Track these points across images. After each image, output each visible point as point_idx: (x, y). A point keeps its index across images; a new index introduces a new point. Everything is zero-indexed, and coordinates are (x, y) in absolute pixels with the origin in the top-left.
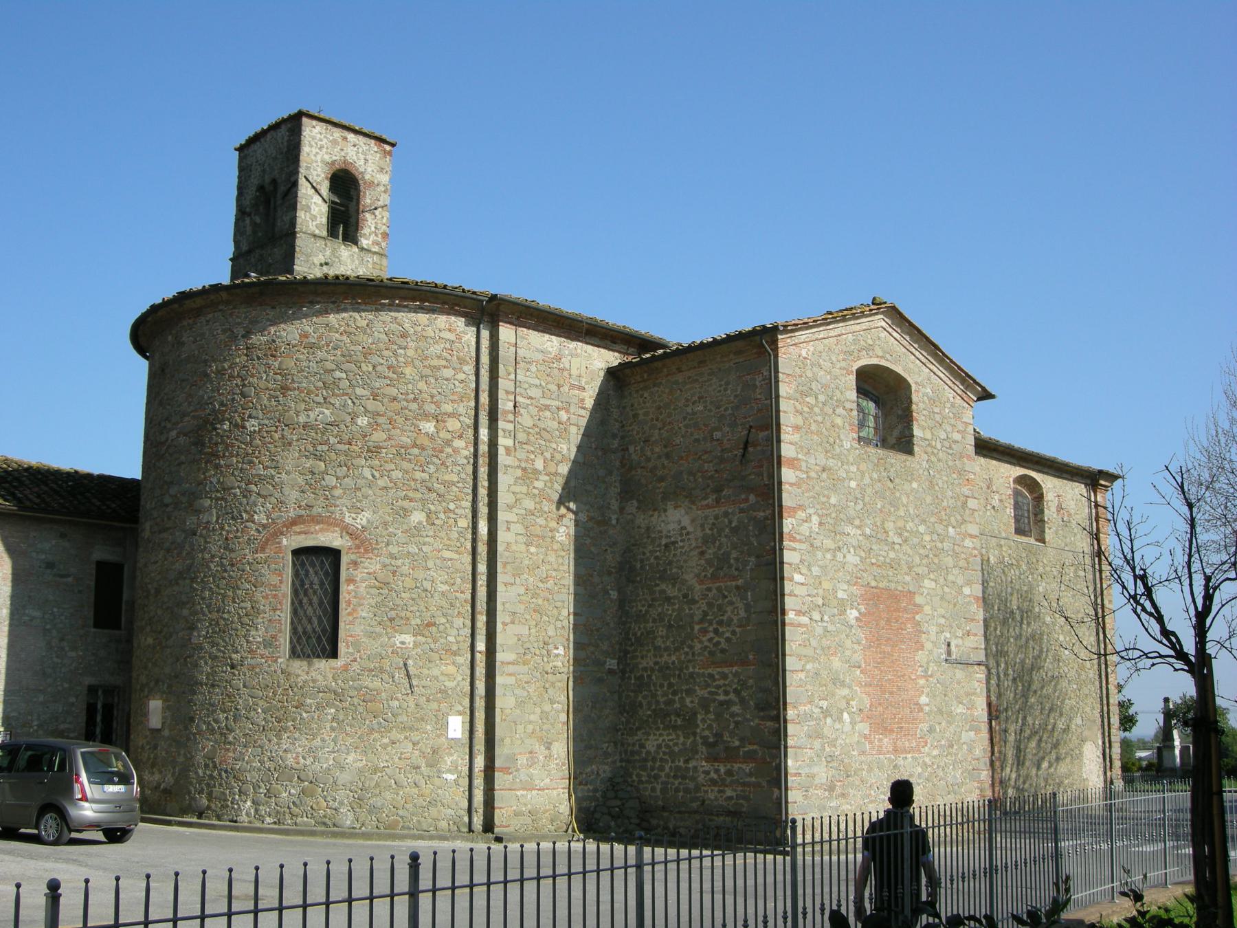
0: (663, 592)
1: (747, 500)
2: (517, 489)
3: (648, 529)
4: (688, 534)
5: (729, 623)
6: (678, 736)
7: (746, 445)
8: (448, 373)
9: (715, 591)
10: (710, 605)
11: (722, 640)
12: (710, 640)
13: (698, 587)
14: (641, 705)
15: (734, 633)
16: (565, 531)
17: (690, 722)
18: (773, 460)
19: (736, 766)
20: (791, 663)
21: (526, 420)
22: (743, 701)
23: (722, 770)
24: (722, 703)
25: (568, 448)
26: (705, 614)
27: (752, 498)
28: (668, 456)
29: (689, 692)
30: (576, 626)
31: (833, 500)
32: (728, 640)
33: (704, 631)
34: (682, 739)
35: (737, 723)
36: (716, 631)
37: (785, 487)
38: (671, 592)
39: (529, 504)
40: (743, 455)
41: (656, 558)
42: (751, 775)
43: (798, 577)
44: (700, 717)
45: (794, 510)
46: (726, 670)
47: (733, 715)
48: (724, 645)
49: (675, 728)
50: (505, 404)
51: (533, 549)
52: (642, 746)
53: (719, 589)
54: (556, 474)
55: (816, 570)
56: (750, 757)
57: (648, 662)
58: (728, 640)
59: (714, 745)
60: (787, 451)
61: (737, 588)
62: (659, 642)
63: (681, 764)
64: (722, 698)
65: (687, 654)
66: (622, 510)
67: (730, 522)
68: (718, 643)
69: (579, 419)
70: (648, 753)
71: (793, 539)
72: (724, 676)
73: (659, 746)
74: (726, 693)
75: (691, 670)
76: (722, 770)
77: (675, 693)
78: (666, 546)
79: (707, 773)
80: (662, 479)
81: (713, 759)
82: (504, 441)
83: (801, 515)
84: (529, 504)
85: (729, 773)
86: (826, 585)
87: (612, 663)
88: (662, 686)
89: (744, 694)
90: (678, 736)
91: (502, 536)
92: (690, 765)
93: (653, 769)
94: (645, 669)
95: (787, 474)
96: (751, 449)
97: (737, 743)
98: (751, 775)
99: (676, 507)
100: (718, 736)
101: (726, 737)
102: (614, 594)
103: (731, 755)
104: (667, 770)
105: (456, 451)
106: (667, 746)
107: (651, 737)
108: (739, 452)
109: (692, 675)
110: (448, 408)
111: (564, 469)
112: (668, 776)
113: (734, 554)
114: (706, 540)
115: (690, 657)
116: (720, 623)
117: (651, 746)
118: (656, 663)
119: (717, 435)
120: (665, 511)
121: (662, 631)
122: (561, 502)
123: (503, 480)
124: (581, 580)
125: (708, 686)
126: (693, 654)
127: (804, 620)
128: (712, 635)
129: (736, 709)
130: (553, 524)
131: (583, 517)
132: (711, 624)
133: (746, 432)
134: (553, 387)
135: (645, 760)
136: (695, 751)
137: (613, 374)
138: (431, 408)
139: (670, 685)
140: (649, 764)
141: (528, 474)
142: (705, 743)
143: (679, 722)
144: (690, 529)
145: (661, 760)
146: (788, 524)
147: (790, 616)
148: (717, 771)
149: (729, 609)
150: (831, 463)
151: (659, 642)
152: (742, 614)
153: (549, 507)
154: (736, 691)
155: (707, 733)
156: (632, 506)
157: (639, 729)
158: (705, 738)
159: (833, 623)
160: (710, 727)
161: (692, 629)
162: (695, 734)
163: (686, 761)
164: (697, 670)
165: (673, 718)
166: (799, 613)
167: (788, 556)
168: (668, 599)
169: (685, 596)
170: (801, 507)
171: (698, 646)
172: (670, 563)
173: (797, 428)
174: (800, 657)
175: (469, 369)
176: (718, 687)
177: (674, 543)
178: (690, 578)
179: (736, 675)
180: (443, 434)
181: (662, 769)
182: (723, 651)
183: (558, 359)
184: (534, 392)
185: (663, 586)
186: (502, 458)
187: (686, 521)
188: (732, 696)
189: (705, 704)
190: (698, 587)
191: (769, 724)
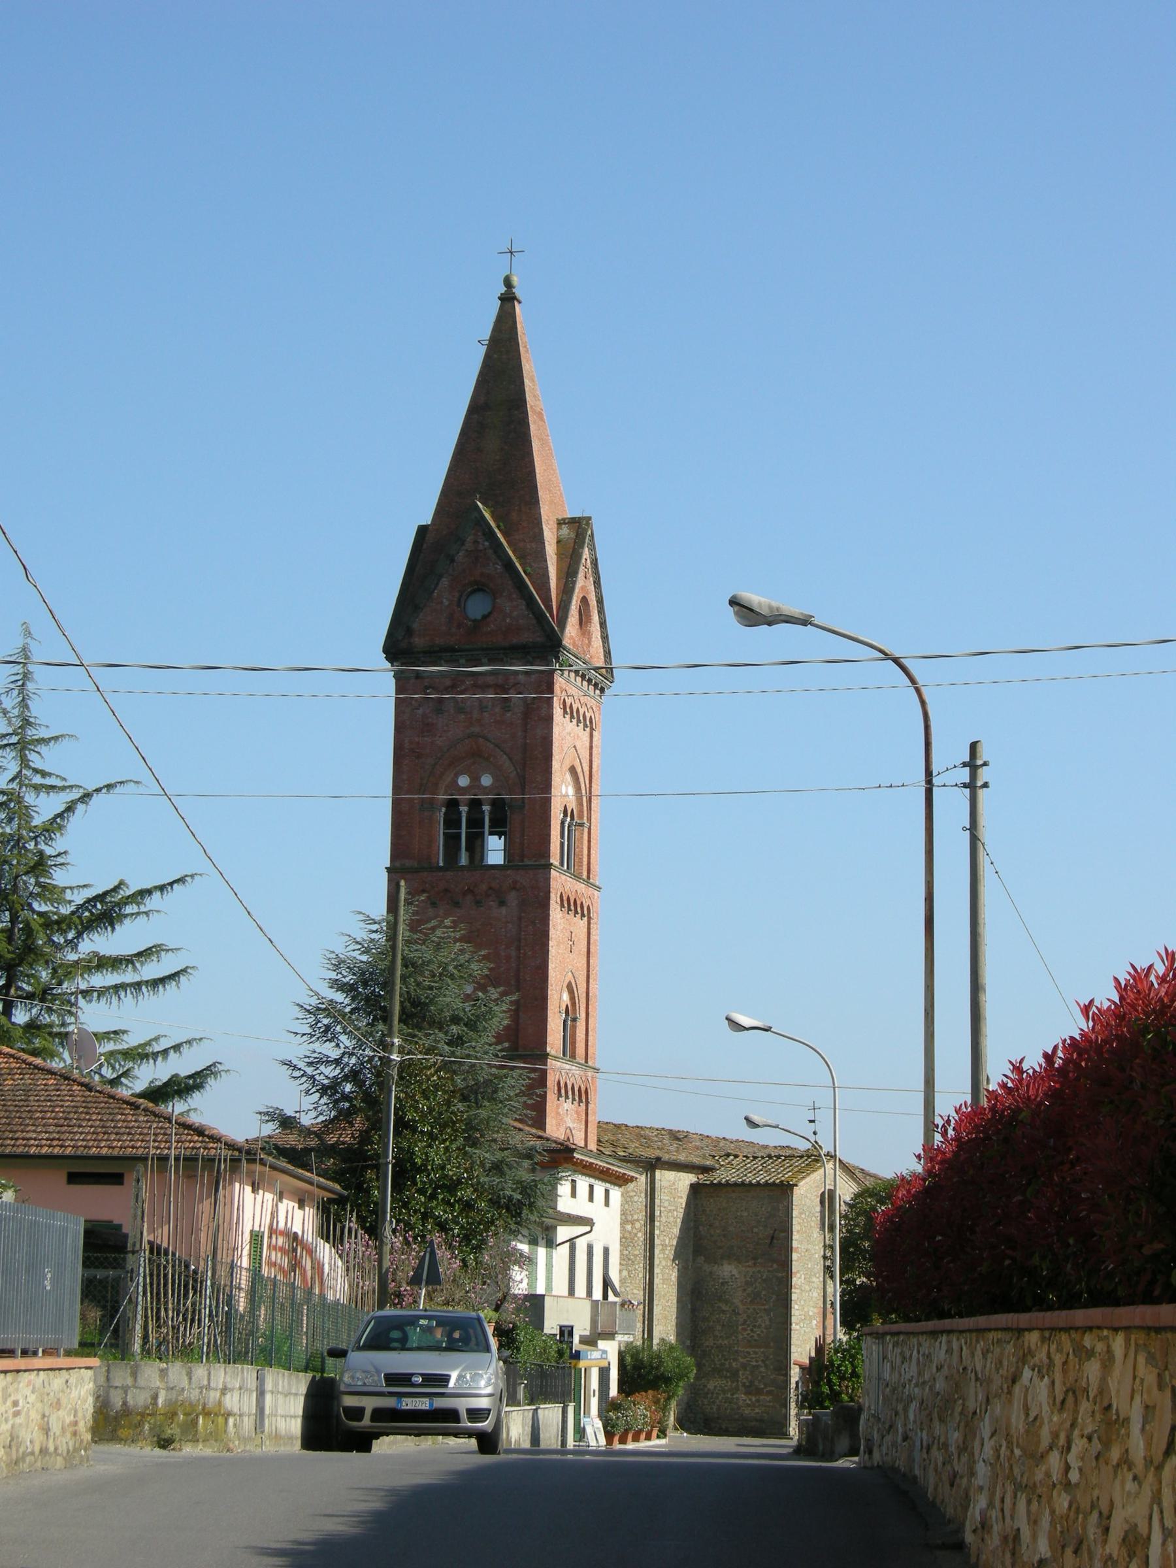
0: (718, 1307)
1: (772, 1266)
2: (660, 1256)
3: (711, 1273)
4: (736, 1278)
5: (760, 1326)
6: (727, 1382)
7: (773, 1238)
8: (636, 1199)
9: (751, 1310)
10: (749, 1317)
11: (755, 1335)
12: (748, 1334)
13: (741, 1307)
14: (704, 1365)
15: (762, 1332)
16: (674, 1275)
17: (735, 1375)
18: (788, 1249)
19: (762, 1397)
20: (793, 1349)
21: (664, 1219)
22: (766, 1366)
23: (754, 1399)
24: (754, 1366)
25: (676, 1231)
26: (745, 1321)
27: (775, 1266)
28: (724, 1236)
29: (735, 1360)
30: (677, 1324)
31: (809, 1266)
32: (758, 1335)
33: (745, 1330)
34: (729, 1383)
35: (763, 1377)
36: (752, 1330)
37: (794, 1263)
38: (724, 1307)
39: (664, 1263)
40: (771, 1243)
41: (716, 1289)
42: (770, 1402)
43: (796, 1307)
44: (741, 1372)
45: (796, 1273)
46: (757, 1350)
47: (761, 1372)
48: (756, 1337)
49: (726, 1377)
50: (657, 1213)
51: (665, 1286)
52: (705, 1386)
53: (754, 1309)
54: (672, 1245)
55: (802, 1302)
56: (769, 1393)
57: (710, 1342)
58: (758, 1335)
59: (748, 1387)
60: (795, 1244)
61: (765, 1309)
62: (717, 1333)
63: (729, 1396)
64: (754, 1363)
65: (734, 1340)
66: (694, 1260)
67: (762, 1276)
68: (753, 1336)
69: (680, 1214)
70: (709, 1390)
71: (795, 1288)
72: (756, 1353)
73: (715, 1387)
74: (757, 1361)
75: (736, 1348)
76: (754, 1399)
77: (726, 1360)
78: (722, 1283)
79: (745, 1400)
80: (720, 1248)
81: (747, 1393)
82: (657, 1232)
83: (798, 1275)
84: (664, 1263)
85: (758, 1401)
86: (806, 1309)
87: (688, 1343)
88: (718, 1356)
89: (767, 1362)
90: (727, 1382)
91: (656, 1281)
92: (735, 1396)
93: (711, 1398)
94: (708, 1346)
95: (795, 1256)
96: (775, 1241)
97: (762, 1386)
98: (770, 1402)
99: (729, 1264)
100: (751, 1382)
101: (756, 1383)
102: (689, 1306)
103: (759, 1392)
104: (720, 1398)
105: (638, 1239)
106: (721, 1387)
107: (711, 1382)
108: (768, 1241)
109: (736, 1351)
110: (636, 1217)
111: (675, 1243)
112: (721, 1402)
113: (763, 1293)
114: (747, 1283)
115: (735, 1342)
116: (754, 1326)
117: (711, 1385)
118: (714, 1344)
119: (755, 1230)
120: (722, 1265)
121: (719, 1327)
122: (674, 1260)
123: (657, 1252)
124: (680, 1300)
125: (746, 1357)
126: (738, 1341)
127: (798, 1327)
128: (749, 1332)
129: (763, 1369)
130: (671, 1272)
131: (680, 1265)
132: (749, 1326)
133: (772, 1232)
134: (672, 1200)
135: (708, 1393)
136: (737, 1389)
137: (695, 1188)
138: (629, 1218)
139: (723, 1355)
140: (709, 1396)
141: (664, 1246)
142: (744, 1385)
143: (728, 1375)
144: (737, 1276)
145: (717, 1393)
146: (794, 1280)
147: (794, 1326)
148: (750, 1400)
149: (760, 1320)
150: (810, 1246)
151: (717, 1333)
152: (767, 1323)
153: (670, 1263)
154: (762, 1361)
155: (745, 1381)
156: (701, 1259)
157: (703, 1377)
158: (744, 1385)
159: (807, 1328)
160: (747, 1378)
161: (737, 1328)
162: (738, 1381)
163: (732, 1395)
164: (740, 1349)
165: (725, 1373)
166: (797, 1324)
167: (794, 1297)
168: (723, 1312)
169: (733, 1311)
170: (798, 1272)
171: (741, 1337)
172: (725, 1292)
173: (798, 1232)
174: (796, 1345)
175: (643, 1195)
176: (753, 1358)
177: (726, 1282)
178: (736, 1301)
179: (763, 1352)
180: (635, 1231)
181: (717, 1398)
182: (755, 1340)
183: (674, 1184)
184: (666, 1204)
185: (720, 1305)
186: (657, 1241)
187: (735, 1272)
188: (760, 1363)
189: (744, 1366)
190: (741, 1307)
191: (782, 1377)
